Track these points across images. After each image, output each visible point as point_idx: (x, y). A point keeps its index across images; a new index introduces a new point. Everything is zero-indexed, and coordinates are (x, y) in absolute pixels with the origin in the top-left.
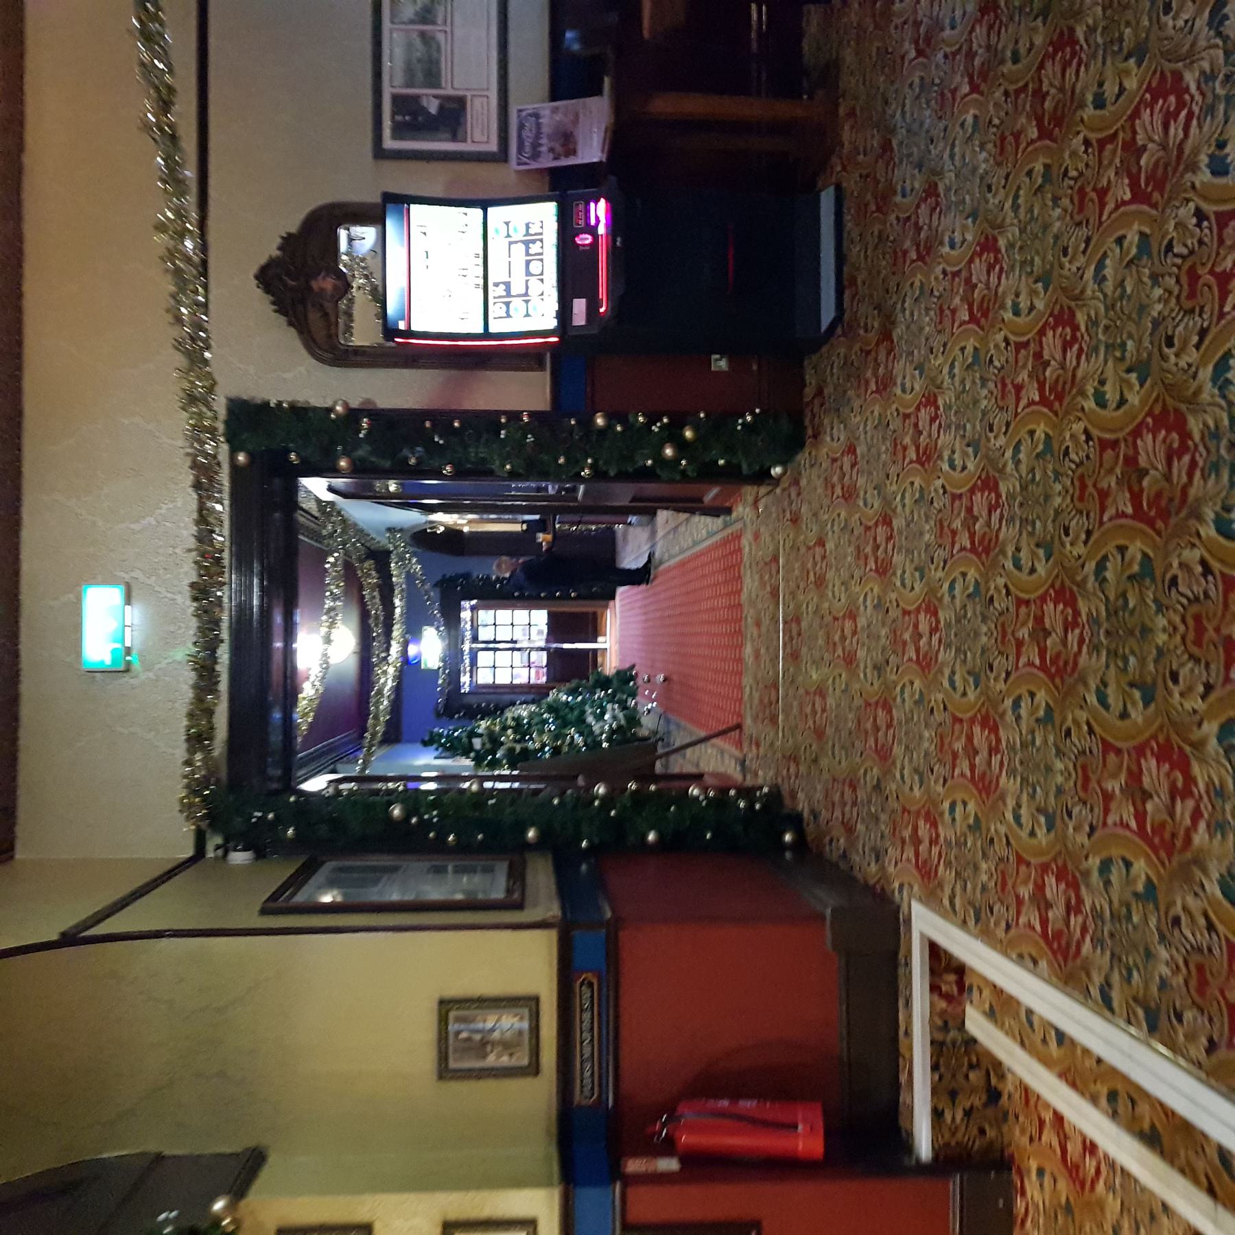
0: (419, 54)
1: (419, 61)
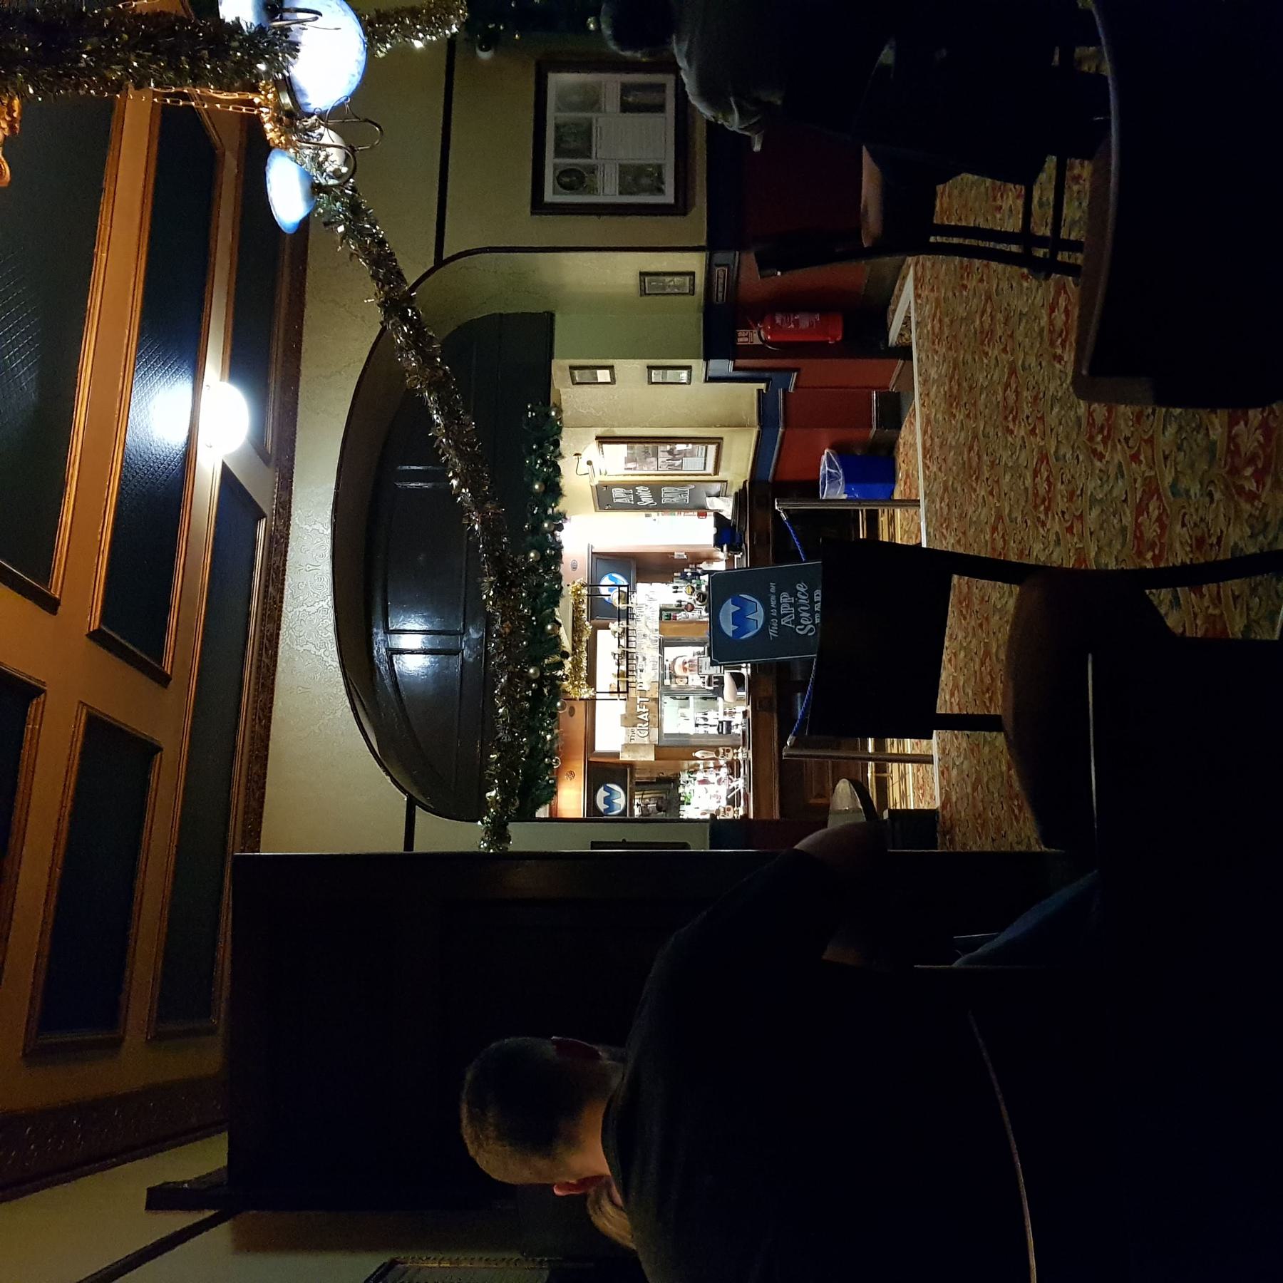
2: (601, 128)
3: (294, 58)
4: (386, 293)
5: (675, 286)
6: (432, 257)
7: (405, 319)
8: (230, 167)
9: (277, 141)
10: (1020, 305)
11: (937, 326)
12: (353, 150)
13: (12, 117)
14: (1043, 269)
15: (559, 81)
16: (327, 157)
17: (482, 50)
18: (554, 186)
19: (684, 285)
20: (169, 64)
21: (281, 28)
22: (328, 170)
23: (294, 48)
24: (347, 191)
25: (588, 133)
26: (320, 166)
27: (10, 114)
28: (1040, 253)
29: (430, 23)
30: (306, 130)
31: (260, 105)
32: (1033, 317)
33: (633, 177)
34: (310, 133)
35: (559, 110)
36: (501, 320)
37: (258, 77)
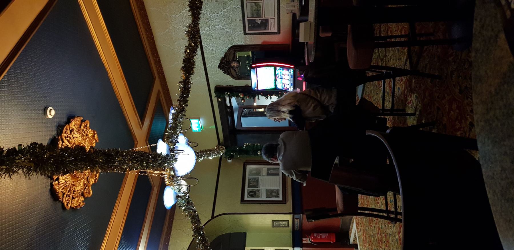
0: (255, 9)
1: (255, 10)
2: (261, 180)
3: (176, 162)
4: (195, 227)
5: (284, 225)
6: (211, 216)
7: (200, 235)
8: (155, 190)
9: (168, 184)
10: (389, 232)
11: (365, 238)
12: (190, 186)
13: (96, 178)
14: (395, 220)
15: (249, 167)
16: (182, 188)
17: (229, 160)
18: (247, 195)
19: (286, 224)
20: (140, 165)
21: (173, 155)
22: (182, 192)
23: (176, 160)
24: (186, 197)
25: (257, 181)
26: (180, 191)
27: (95, 177)
28: (393, 216)
29: (214, 153)
30: (177, 181)
31: (164, 175)
32: (394, 236)
33: (271, 193)
34: (178, 182)
35: (249, 175)
36: (230, 236)
37: (165, 167)
